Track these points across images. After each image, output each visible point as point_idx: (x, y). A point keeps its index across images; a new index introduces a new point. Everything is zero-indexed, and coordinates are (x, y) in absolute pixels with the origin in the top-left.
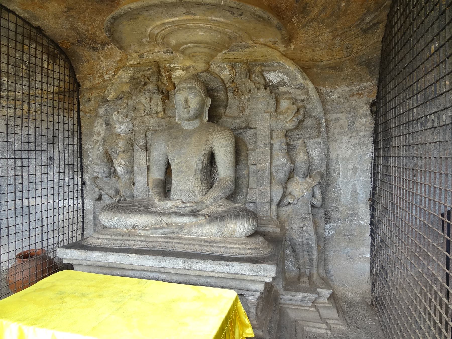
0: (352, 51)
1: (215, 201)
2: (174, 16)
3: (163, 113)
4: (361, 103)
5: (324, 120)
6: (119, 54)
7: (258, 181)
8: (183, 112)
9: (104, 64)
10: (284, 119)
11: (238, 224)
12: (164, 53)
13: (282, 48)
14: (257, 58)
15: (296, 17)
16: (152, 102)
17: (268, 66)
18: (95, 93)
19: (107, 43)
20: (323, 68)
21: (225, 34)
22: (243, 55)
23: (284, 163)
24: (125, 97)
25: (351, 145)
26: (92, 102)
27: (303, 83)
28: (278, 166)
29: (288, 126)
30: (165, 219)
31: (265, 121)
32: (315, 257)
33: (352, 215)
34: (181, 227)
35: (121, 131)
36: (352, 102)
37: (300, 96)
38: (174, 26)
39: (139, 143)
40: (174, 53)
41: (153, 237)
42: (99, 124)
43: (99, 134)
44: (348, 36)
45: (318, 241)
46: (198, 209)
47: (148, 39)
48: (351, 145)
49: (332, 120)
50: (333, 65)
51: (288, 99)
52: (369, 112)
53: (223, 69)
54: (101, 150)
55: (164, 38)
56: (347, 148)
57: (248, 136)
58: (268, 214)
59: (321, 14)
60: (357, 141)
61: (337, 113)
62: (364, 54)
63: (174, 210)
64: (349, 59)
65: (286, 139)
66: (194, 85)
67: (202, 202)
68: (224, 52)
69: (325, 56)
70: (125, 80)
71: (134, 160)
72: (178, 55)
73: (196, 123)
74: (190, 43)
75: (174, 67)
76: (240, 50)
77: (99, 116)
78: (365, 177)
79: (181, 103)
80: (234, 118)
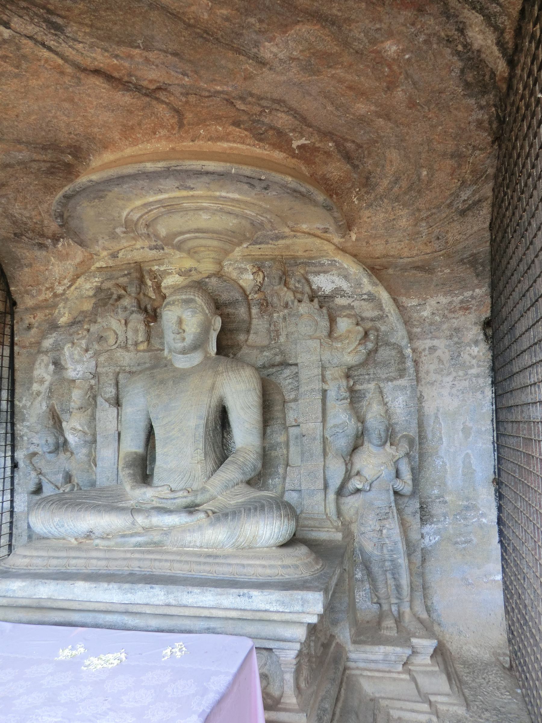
0: (447, 243)
1: (227, 487)
2: (160, 191)
3: (146, 344)
4: (468, 323)
5: (409, 350)
6: (79, 254)
7: (303, 454)
8: (174, 339)
9: (56, 269)
10: (343, 349)
11: (261, 524)
12: (151, 249)
13: (337, 240)
14: (298, 254)
15: (357, 193)
16: (129, 326)
18: (40, 315)
19: (61, 237)
20: (404, 269)
21: (245, 217)
22: (275, 249)
23: (345, 422)
24: (87, 320)
27: (372, 292)
28: (335, 426)
29: (350, 359)
30: (140, 520)
31: (315, 356)
32: (405, 581)
33: (467, 508)
34: (168, 531)
36: (454, 320)
37: (369, 313)
38: (163, 207)
40: (165, 248)
41: (118, 551)
42: (43, 365)
43: (42, 381)
45: (409, 555)
46: (198, 501)
47: (124, 229)
49: (424, 350)
50: (420, 264)
51: (348, 316)
52: (481, 337)
53: (243, 271)
54: (44, 408)
55: (147, 226)
56: (451, 395)
57: (285, 379)
58: (322, 508)
59: (392, 187)
60: (466, 383)
61: (431, 339)
62: (465, 247)
63: (156, 504)
64: (443, 255)
65: (348, 381)
66: (192, 297)
67: (204, 490)
68: (245, 246)
69: (406, 250)
70: (87, 293)
71: (97, 422)
72: (171, 251)
73: (197, 358)
74: (189, 232)
75: (165, 270)
76: (271, 242)
77: (43, 352)
78: (483, 443)
80: (262, 349)
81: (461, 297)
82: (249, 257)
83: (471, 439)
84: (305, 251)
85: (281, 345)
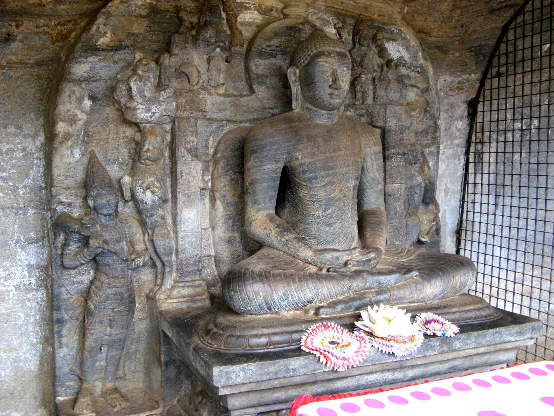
0: (466, 31)
4: (460, 101)
8: (331, 94)
16: (212, 64)
17: (387, 33)
18: (28, 25)
22: (356, 6)
25: (446, 157)
26: (17, 43)
27: (424, 66)
35: (151, 117)
36: (451, 97)
39: (187, 142)
42: (74, 98)
43: (72, 121)
44: (470, 12)
48: (446, 157)
50: (441, 44)
52: (466, 114)
53: (326, 23)
60: (451, 151)
62: (477, 38)
64: (459, 41)
69: (436, 30)
70: (138, 11)
77: (73, 81)
78: (455, 201)
79: (326, 78)
81: (460, 79)
82: (331, 9)
83: (448, 198)
84: (380, 15)
85: (369, 107)
